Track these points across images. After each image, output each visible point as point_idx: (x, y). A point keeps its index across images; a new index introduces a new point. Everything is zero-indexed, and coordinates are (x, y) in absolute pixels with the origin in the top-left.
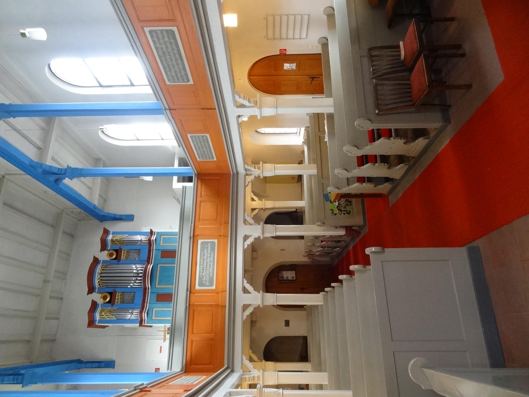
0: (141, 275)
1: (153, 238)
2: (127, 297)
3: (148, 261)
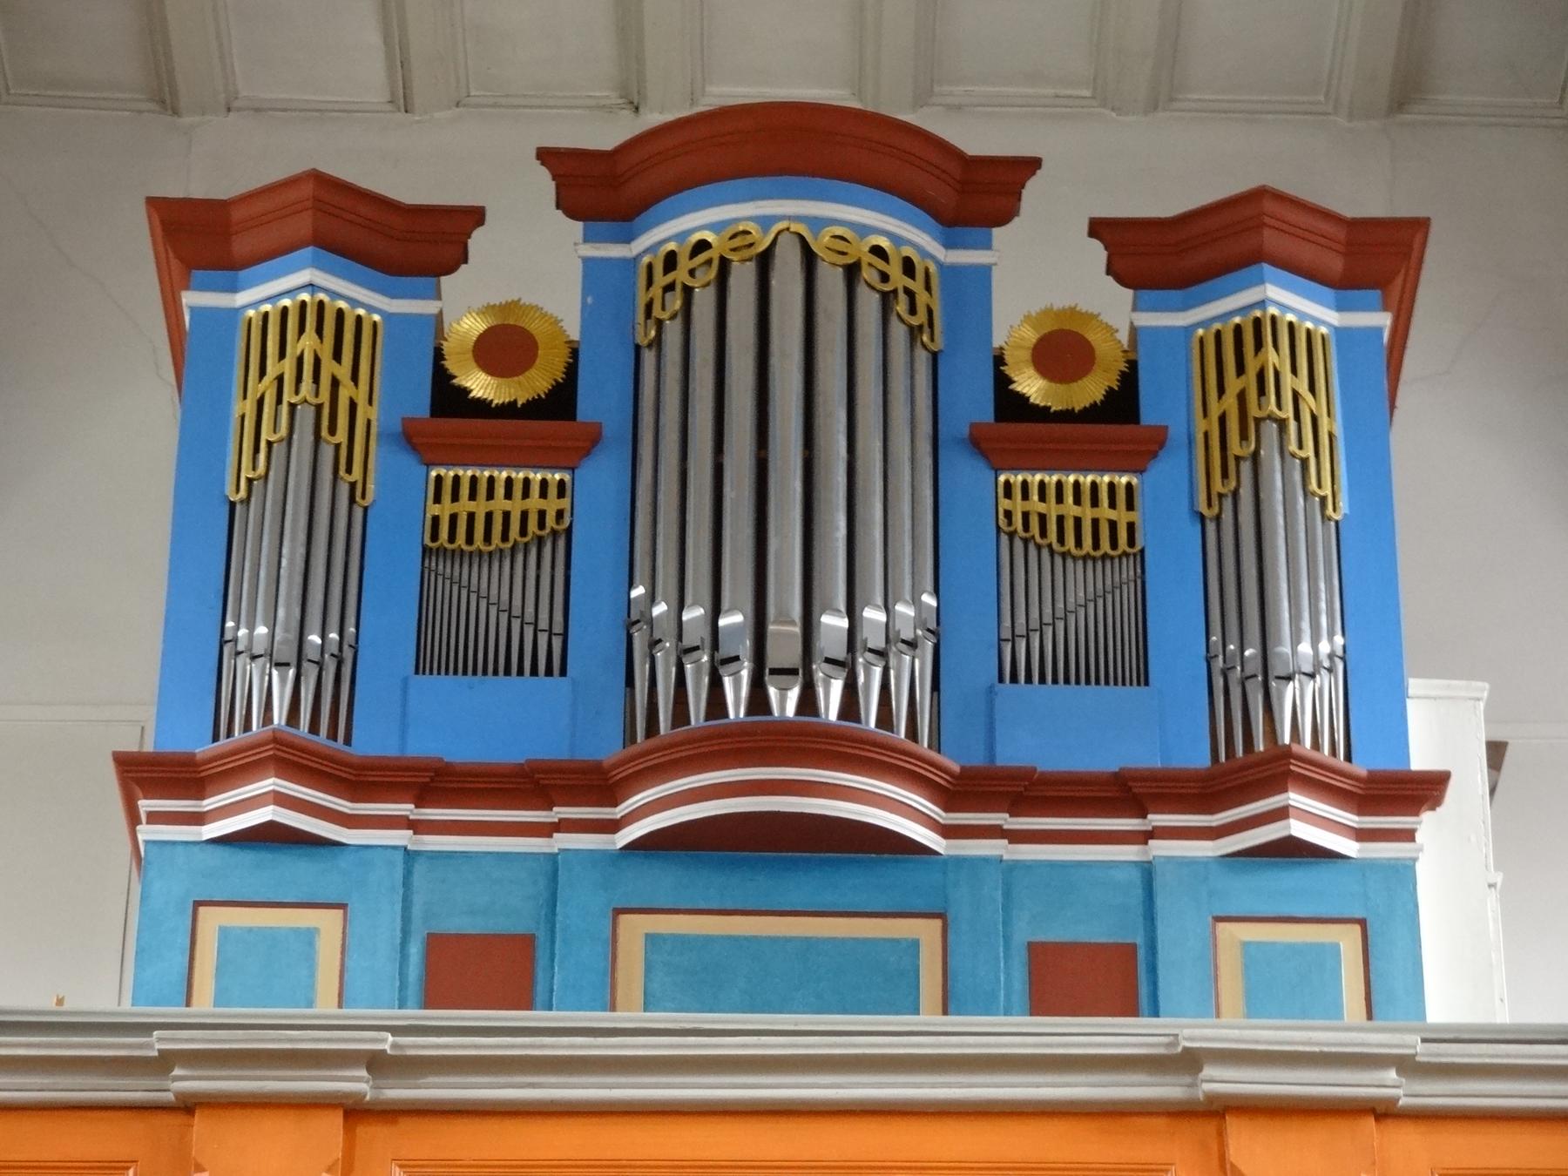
0: (785, 702)
2: (501, 592)
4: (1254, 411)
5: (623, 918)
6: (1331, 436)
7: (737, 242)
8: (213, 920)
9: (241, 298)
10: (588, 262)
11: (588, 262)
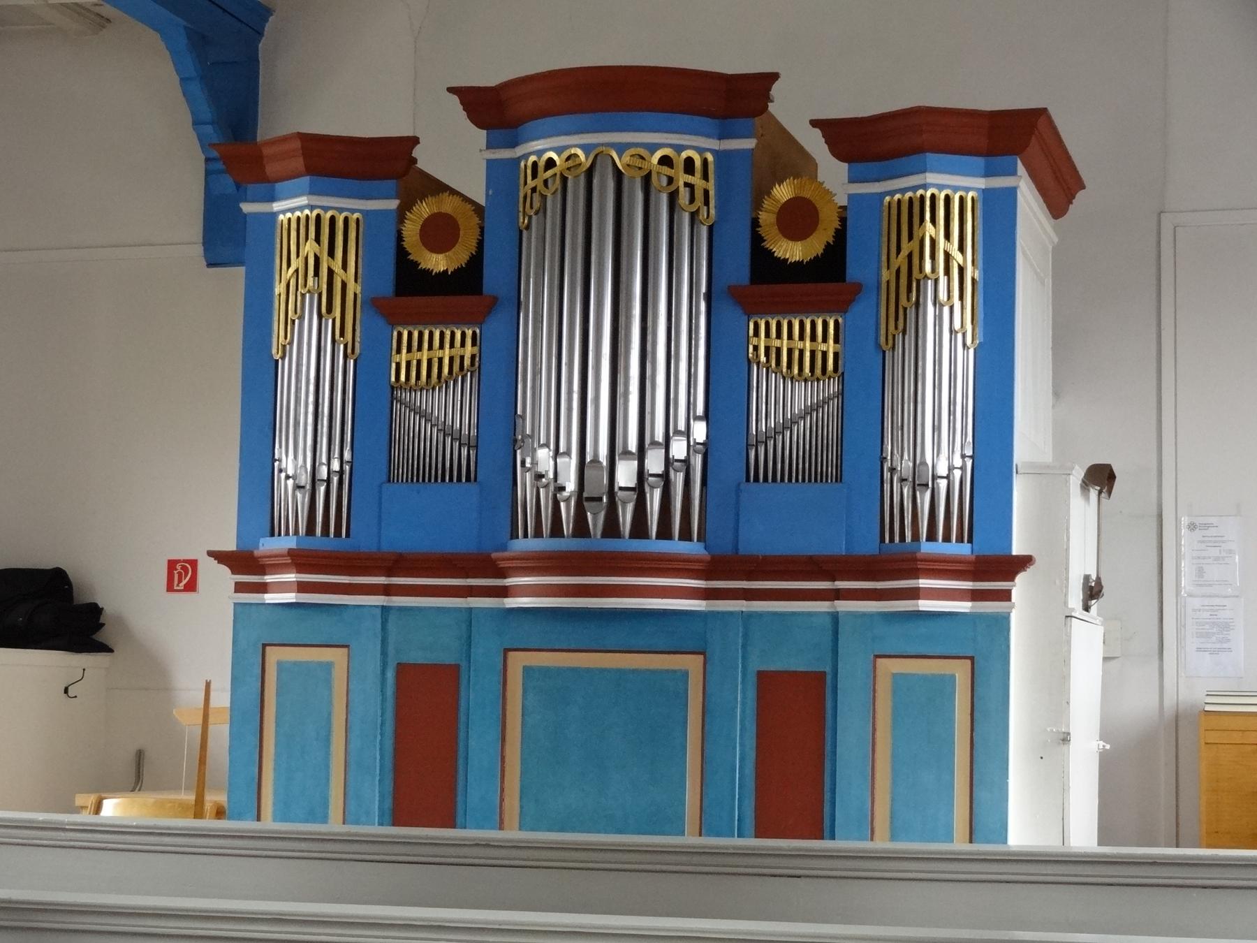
0: (596, 520)
1: (941, 599)
3: (726, 567)
4: (916, 274)
5: (511, 654)
6: (973, 279)
7: (570, 163)
8: (274, 655)
9: (277, 206)
10: (489, 161)
11: (489, 161)
